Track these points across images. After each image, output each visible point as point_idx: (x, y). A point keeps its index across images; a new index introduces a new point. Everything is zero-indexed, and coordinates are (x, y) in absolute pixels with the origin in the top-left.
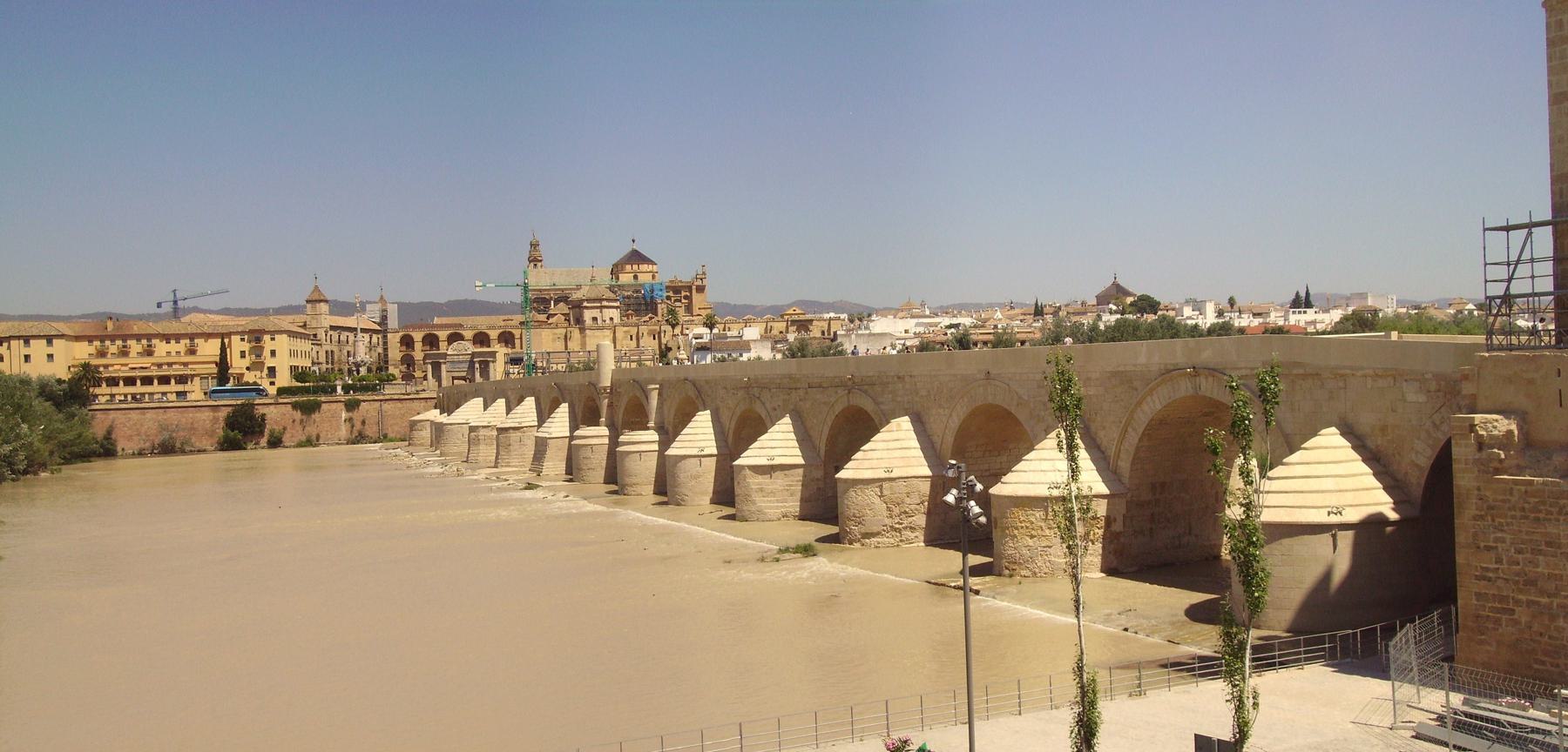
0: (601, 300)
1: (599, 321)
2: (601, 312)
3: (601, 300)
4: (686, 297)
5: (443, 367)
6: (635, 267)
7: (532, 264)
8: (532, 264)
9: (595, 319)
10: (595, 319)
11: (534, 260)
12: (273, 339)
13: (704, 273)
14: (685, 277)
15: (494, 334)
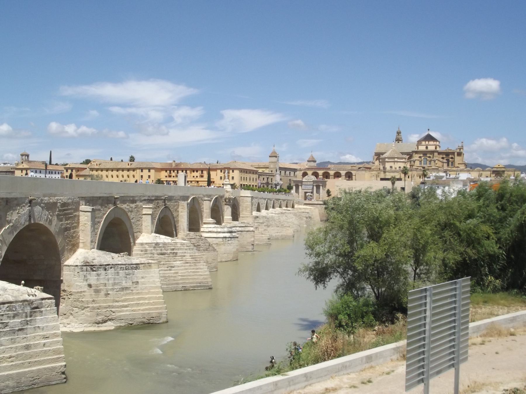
0: (394, 158)
1: (393, 168)
2: (394, 164)
3: (394, 158)
4: (452, 158)
5: (300, 187)
6: (427, 143)
7: (397, 142)
8: (397, 142)
9: (391, 167)
10: (391, 167)
11: (398, 140)
12: (233, 172)
13: (462, 146)
14: (453, 148)
15: (343, 173)
